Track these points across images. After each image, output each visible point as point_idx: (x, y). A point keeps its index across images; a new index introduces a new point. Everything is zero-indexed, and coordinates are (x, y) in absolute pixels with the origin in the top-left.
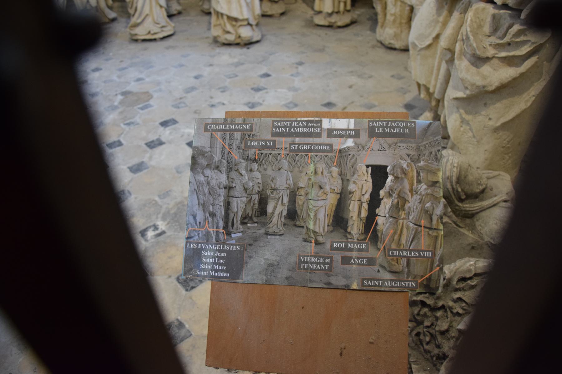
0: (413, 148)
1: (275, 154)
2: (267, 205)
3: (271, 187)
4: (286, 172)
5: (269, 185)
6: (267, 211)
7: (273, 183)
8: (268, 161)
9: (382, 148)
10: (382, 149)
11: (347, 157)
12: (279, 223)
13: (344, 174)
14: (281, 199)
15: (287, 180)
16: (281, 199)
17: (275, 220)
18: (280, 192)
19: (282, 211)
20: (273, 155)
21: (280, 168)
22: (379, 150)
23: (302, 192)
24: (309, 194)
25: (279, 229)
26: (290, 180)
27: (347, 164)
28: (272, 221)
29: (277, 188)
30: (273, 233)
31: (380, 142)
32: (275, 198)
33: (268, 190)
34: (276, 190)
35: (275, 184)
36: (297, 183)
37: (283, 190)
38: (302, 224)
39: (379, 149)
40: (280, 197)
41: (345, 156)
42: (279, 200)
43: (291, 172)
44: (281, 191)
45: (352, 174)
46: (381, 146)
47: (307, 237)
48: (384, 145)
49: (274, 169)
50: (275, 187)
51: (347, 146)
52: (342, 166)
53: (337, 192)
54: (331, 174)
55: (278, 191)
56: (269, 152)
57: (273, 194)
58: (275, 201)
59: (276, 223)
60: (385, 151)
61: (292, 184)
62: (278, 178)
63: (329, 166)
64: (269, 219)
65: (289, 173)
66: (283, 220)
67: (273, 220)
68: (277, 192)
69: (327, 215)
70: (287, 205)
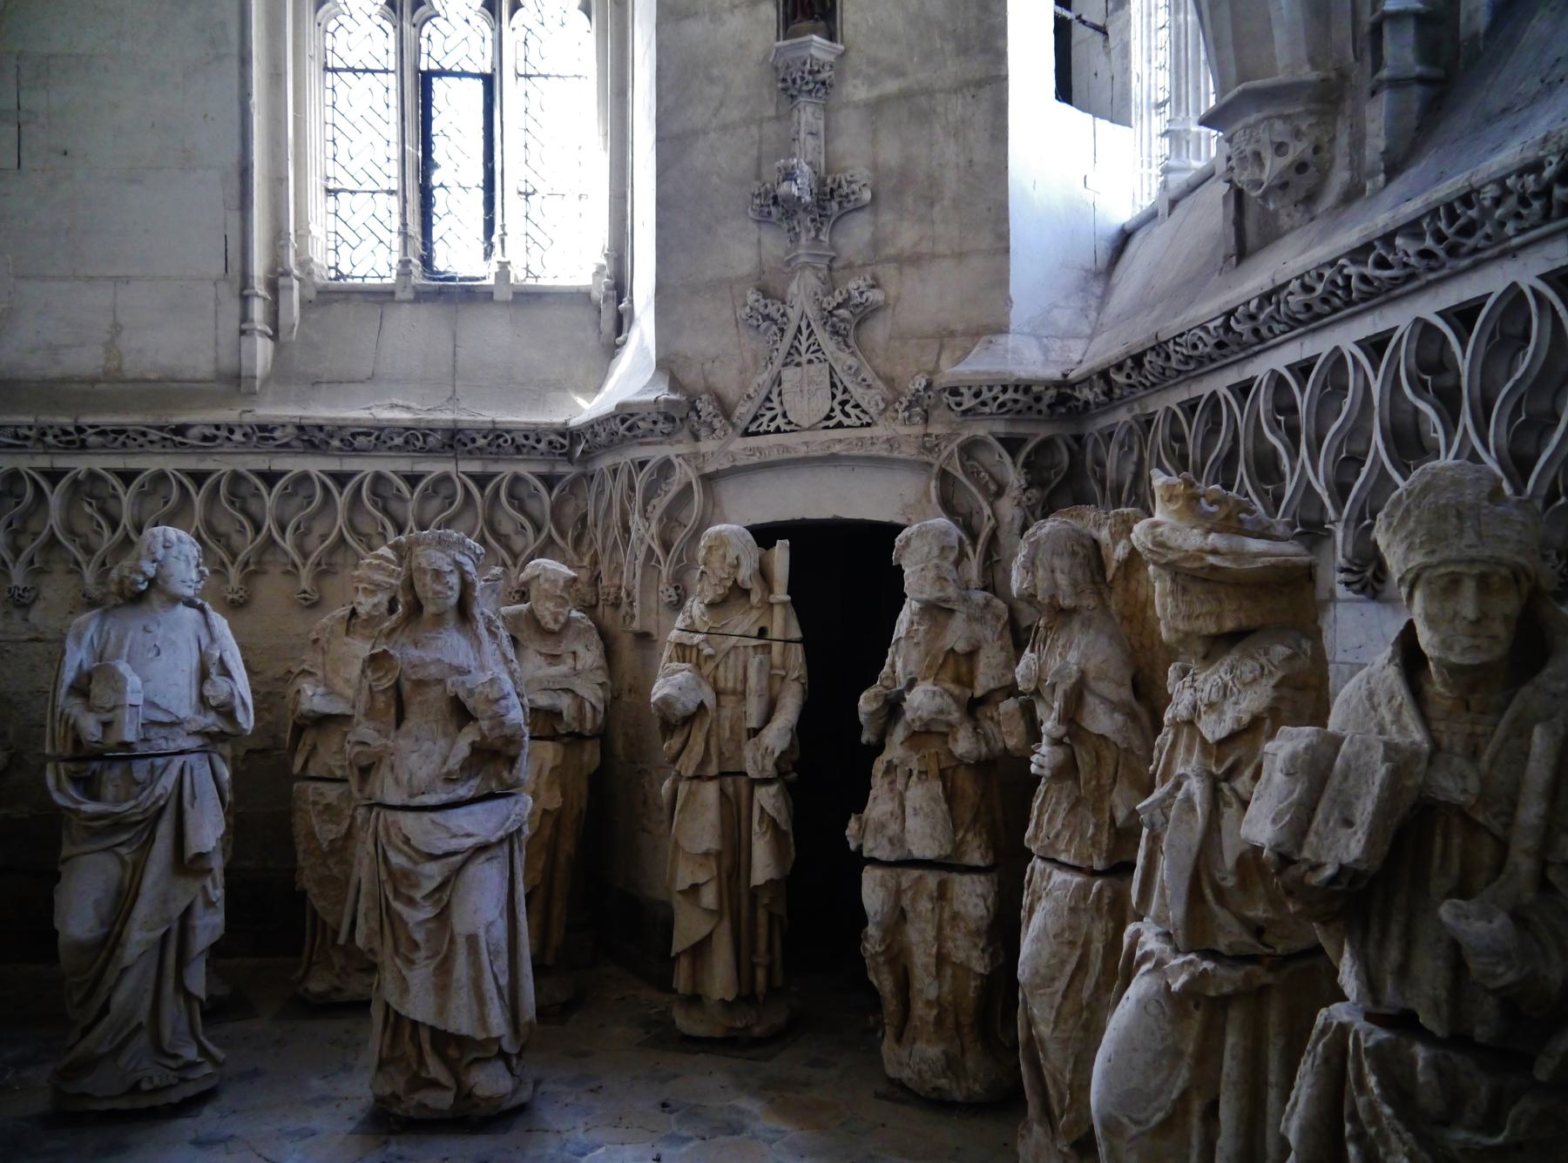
0: (1038, 399)
1: (93, 476)
2: (56, 877)
3: (77, 742)
4: (192, 614)
5: (60, 730)
6: (55, 934)
7: (90, 709)
8: (36, 534)
9: (848, 408)
10: (847, 415)
11: (623, 478)
12: (172, 1008)
13: (611, 597)
14: (165, 829)
15: (204, 675)
16: (165, 829)
17: (129, 994)
18: (154, 776)
19: (187, 913)
20: (76, 483)
21: (143, 587)
22: (831, 423)
23: (331, 755)
24: (384, 770)
25: (175, 1057)
26: (226, 672)
27: (626, 529)
28: (105, 1009)
29: (127, 745)
30: (123, 1104)
31: (831, 366)
32: (118, 824)
33: (50, 767)
34: (126, 754)
35: (106, 717)
36: (291, 692)
37: (182, 752)
38: (355, 987)
39: (829, 418)
40: (163, 808)
41: (615, 472)
42: (151, 839)
43: (235, 607)
44: (165, 768)
45: (668, 593)
46: (840, 397)
47: (400, 1083)
48: (857, 393)
49: (95, 593)
50: (112, 740)
51: (621, 406)
52: (599, 546)
53: (576, 727)
54: (523, 607)
55: (140, 770)
56: (43, 462)
57: (95, 797)
58: (123, 851)
59: (143, 1016)
60: (866, 432)
61: (249, 701)
62: (123, 667)
63: (509, 549)
64: (77, 997)
65: (220, 623)
66: (197, 980)
67: (120, 997)
68: (129, 771)
69: (528, 897)
70: (217, 864)
